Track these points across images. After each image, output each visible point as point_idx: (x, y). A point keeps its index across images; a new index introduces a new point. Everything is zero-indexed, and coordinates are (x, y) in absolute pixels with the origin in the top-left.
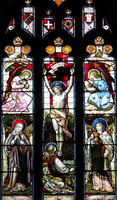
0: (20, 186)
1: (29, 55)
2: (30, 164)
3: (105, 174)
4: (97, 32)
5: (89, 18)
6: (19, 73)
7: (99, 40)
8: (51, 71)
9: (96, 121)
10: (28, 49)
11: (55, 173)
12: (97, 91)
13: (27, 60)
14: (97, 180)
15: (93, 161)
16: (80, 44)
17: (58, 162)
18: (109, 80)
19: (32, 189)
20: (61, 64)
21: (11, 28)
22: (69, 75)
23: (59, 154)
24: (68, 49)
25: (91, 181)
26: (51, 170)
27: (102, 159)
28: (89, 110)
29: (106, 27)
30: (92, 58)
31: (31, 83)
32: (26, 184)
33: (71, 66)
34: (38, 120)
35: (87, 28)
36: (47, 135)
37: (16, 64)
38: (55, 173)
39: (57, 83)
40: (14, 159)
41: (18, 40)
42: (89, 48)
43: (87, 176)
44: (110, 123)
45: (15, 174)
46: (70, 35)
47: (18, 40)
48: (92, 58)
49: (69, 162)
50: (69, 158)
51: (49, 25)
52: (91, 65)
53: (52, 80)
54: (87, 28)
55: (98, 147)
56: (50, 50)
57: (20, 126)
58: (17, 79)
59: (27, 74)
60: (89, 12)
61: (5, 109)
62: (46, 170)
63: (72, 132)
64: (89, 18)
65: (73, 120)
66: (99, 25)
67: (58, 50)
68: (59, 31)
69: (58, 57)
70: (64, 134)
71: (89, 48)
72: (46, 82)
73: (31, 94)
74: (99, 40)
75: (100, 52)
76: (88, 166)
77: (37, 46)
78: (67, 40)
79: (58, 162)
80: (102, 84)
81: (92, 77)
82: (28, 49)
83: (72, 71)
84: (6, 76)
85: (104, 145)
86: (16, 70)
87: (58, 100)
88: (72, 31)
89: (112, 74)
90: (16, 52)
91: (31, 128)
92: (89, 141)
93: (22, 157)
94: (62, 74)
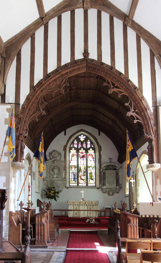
0: (74, 182)
1: (76, 152)
2: (76, 177)
3: (92, 179)
4: (91, 147)
5: (89, 144)
6: (74, 156)
7: (91, 149)
8: (81, 156)
9: (90, 167)
10: (75, 151)
11: (81, 179)
12: (91, 161)
13: (75, 153)
14: (91, 180)
15: (90, 176)
16: (87, 150)
17: (82, 176)
18: (93, 158)
19: (77, 182)
20: (83, 154)
21: (72, 146)
22: (84, 157)
23: (83, 175)
24: (84, 151)
25: (89, 181)
26: (81, 178)
27: (92, 176)
28: (89, 165)
29: (93, 146)
30: (89, 153)
31: (76, 159)
32: (75, 181)
33: (85, 155)
34: (78, 167)
35: (89, 146)
36: (80, 171)
37: (73, 154)
38: (81, 179)
39: (82, 159)
40: (73, 176)
41: (73, 149)
42: (89, 151)
43: (88, 180)
44: (93, 168)
45: (73, 179)
46: (85, 148)
47: (73, 149)
48: (89, 153)
49: (85, 177)
50: (85, 176)
51: (80, 145)
52: (89, 155)
53: (81, 158)
54: (89, 146)
55: (91, 173)
56: (80, 151)
57: (74, 168)
58: (73, 158)
59: (75, 156)
60: (89, 143)
61: (71, 164)
62: (80, 178)
63: (85, 170)
64: (89, 144)
65: (85, 167)
66: (91, 146)
67: (82, 151)
68: (82, 147)
69: (82, 153)
70: (84, 170)
71: (89, 151)
72: (79, 158)
73: (76, 161)
74: (91, 149)
75: (91, 152)
76: (89, 177)
77: (78, 150)
78: (84, 149)
79: (82, 176)
80: (92, 159)
81: (90, 158)
82: (75, 151)
83: (85, 156)
84: (71, 157)
85: (92, 173)
86: (73, 155)
87: (82, 163)
88: (85, 147)
89: (94, 157)
90: (73, 151)
91: (76, 169)
92: (89, 172)
93: (74, 175)
94: (83, 157)
